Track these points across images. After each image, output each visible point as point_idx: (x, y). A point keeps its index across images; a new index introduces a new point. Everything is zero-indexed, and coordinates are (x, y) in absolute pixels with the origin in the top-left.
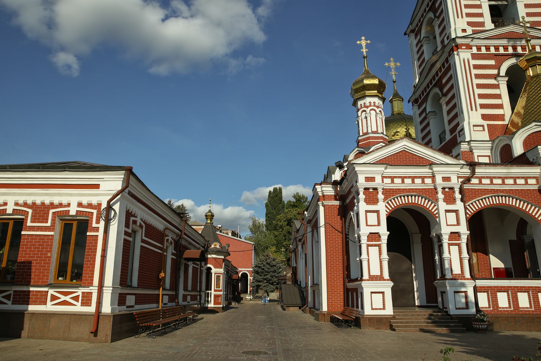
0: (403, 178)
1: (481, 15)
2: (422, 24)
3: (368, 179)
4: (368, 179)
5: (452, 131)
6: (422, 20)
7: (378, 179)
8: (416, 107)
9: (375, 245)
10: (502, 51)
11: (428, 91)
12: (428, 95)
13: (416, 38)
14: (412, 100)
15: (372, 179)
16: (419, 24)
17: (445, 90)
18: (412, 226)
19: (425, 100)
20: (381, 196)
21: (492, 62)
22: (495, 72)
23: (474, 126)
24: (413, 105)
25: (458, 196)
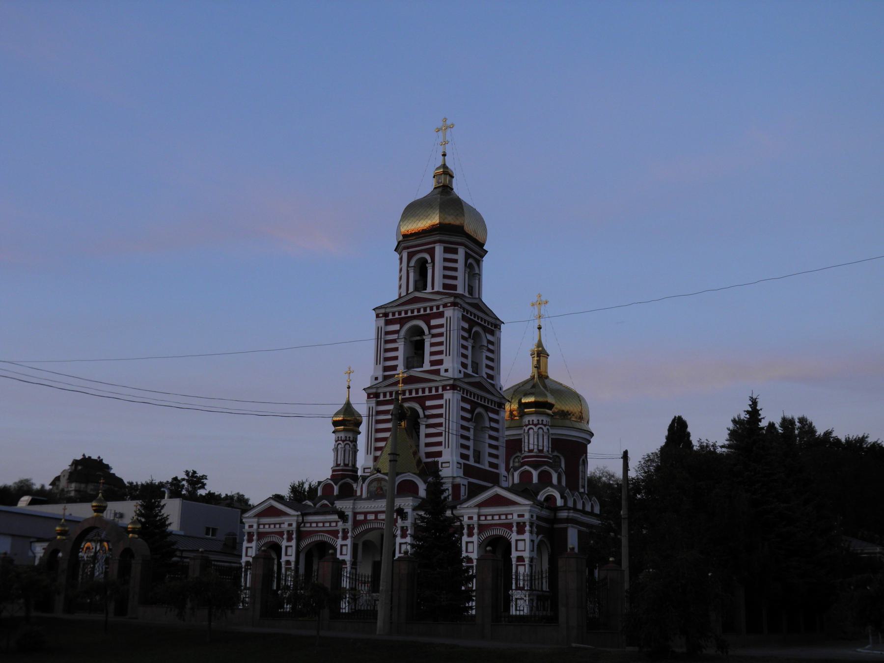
0: (270, 524)
1: (396, 358)
7: (255, 527)
20: (255, 537)
25: (294, 536)
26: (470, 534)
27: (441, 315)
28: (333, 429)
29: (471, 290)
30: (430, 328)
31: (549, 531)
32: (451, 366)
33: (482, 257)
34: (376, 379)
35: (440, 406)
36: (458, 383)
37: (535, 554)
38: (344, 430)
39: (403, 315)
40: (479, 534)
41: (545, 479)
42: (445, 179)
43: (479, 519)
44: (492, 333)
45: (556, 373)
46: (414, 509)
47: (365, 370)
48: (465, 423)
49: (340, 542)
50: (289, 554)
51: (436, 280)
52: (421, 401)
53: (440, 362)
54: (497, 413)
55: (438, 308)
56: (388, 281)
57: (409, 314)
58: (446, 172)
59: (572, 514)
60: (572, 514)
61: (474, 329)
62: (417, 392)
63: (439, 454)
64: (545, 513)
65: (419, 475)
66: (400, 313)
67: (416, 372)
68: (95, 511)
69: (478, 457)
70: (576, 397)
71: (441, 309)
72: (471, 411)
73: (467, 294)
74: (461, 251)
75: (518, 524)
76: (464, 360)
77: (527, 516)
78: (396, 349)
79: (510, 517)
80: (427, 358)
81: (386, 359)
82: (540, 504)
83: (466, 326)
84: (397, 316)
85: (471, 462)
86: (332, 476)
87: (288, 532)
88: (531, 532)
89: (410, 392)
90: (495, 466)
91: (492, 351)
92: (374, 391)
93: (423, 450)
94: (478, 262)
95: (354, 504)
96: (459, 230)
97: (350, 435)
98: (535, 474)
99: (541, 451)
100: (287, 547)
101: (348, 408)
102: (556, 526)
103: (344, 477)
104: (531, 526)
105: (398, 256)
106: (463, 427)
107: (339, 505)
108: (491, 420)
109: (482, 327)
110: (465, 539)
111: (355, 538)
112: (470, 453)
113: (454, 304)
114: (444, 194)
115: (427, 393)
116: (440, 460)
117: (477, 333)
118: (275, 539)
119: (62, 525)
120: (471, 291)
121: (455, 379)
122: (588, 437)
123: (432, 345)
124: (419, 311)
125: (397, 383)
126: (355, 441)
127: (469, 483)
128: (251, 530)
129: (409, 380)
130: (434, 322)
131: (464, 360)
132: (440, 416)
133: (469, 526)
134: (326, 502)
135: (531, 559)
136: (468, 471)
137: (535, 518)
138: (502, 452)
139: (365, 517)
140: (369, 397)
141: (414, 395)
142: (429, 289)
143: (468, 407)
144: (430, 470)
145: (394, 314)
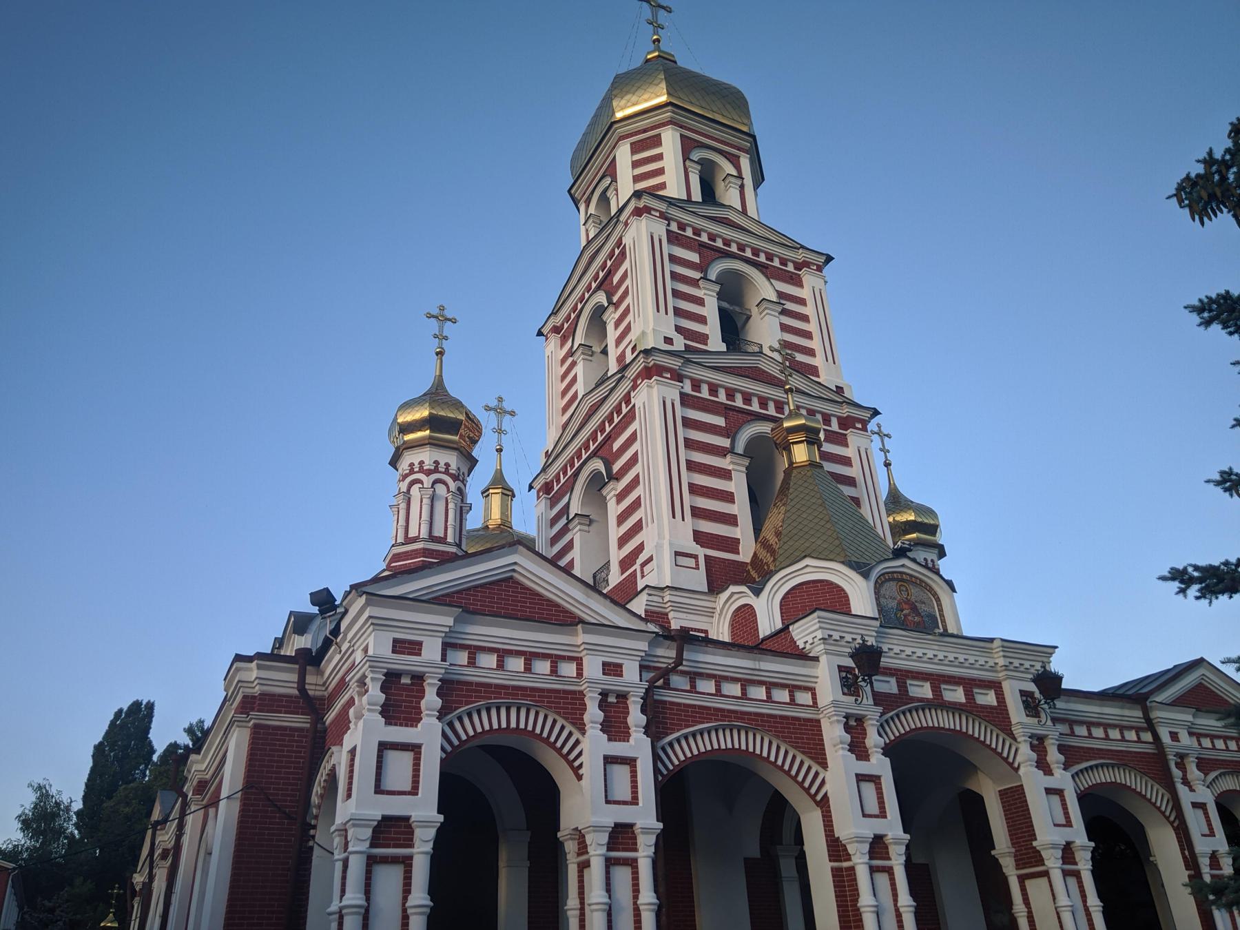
0: (502, 654)
2: (578, 316)
3: (400, 646)
4: (400, 646)
5: (626, 563)
6: (579, 306)
7: (432, 650)
8: (543, 504)
9: (394, 860)
10: (739, 402)
11: (577, 465)
12: (576, 475)
13: (562, 345)
14: (537, 486)
15: (413, 648)
16: (573, 316)
17: (616, 467)
18: (507, 805)
19: (569, 487)
20: (431, 700)
21: (720, 421)
22: (725, 442)
23: (677, 554)
24: (538, 498)
25: (636, 717)
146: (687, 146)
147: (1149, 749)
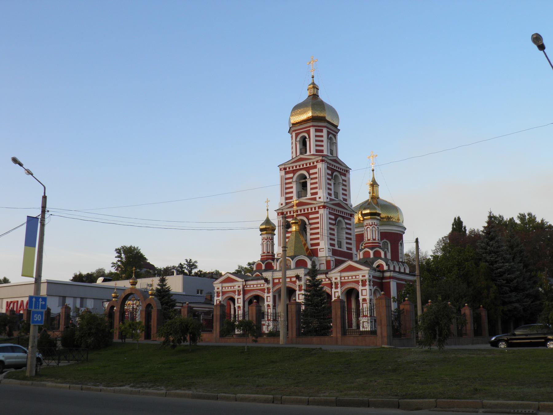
1: (292, 192)
7: (220, 289)
20: (221, 294)
25: (241, 293)
26: (336, 288)
27: (315, 167)
28: (260, 233)
29: (332, 152)
30: (310, 174)
31: (380, 284)
32: (322, 195)
33: (337, 133)
34: (282, 204)
35: (317, 218)
36: (325, 204)
37: (372, 297)
38: (266, 233)
39: (294, 168)
40: (341, 287)
41: (377, 255)
42: (314, 91)
43: (341, 279)
44: (345, 175)
45: (384, 195)
46: (305, 275)
47: (276, 200)
48: (332, 227)
49: (266, 295)
50: (239, 302)
51: (312, 147)
52: (307, 215)
53: (316, 193)
54: (350, 219)
55: (313, 163)
56: (285, 150)
57: (298, 168)
58: (315, 87)
59: (392, 274)
60: (392, 274)
61: (335, 174)
62: (304, 211)
63: (318, 244)
64: (377, 274)
65: (308, 256)
66: (293, 167)
67: (303, 200)
68: (132, 285)
69: (340, 245)
70: (395, 209)
71: (315, 164)
72: (335, 220)
73: (329, 154)
74: (325, 131)
75: (362, 281)
76: (330, 192)
77: (367, 277)
78: (292, 187)
79: (357, 277)
80: (309, 191)
81: (287, 193)
82: (374, 270)
83: (330, 172)
84: (291, 169)
85: (336, 248)
86: (261, 259)
87: (238, 290)
88: (370, 285)
89: (301, 211)
90: (350, 249)
91: (345, 186)
92: (281, 211)
93: (309, 242)
94: (335, 136)
95: (272, 274)
96: (323, 119)
97: (270, 236)
98: (372, 253)
99: (375, 240)
100: (238, 299)
101: (268, 221)
102: (384, 281)
103: (267, 259)
104: (370, 281)
105: (290, 136)
106: (331, 229)
107: (265, 275)
108: (346, 223)
109: (338, 172)
110: (334, 290)
111: (274, 292)
112: (335, 243)
113: (322, 161)
114: (314, 100)
115: (310, 211)
116: (319, 247)
117: (336, 176)
118: (232, 295)
119: (115, 293)
120: (332, 152)
121: (325, 202)
122: (403, 230)
123: (311, 184)
124: (303, 165)
125: (293, 206)
126: (272, 239)
127: (335, 259)
128: (218, 290)
129: (298, 205)
130: (311, 171)
131: (330, 192)
132: (318, 223)
133: (335, 283)
134: (258, 273)
135: (371, 300)
136: (335, 253)
137: (371, 277)
138: (353, 242)
139: (279, 281)
140: (278, 215)
141: (303, 212)
142: (308, 153)
143: (333, 217)
144: (313, 254)
145: (289, 168)
146: (297, 135)
147: (330, 282)
